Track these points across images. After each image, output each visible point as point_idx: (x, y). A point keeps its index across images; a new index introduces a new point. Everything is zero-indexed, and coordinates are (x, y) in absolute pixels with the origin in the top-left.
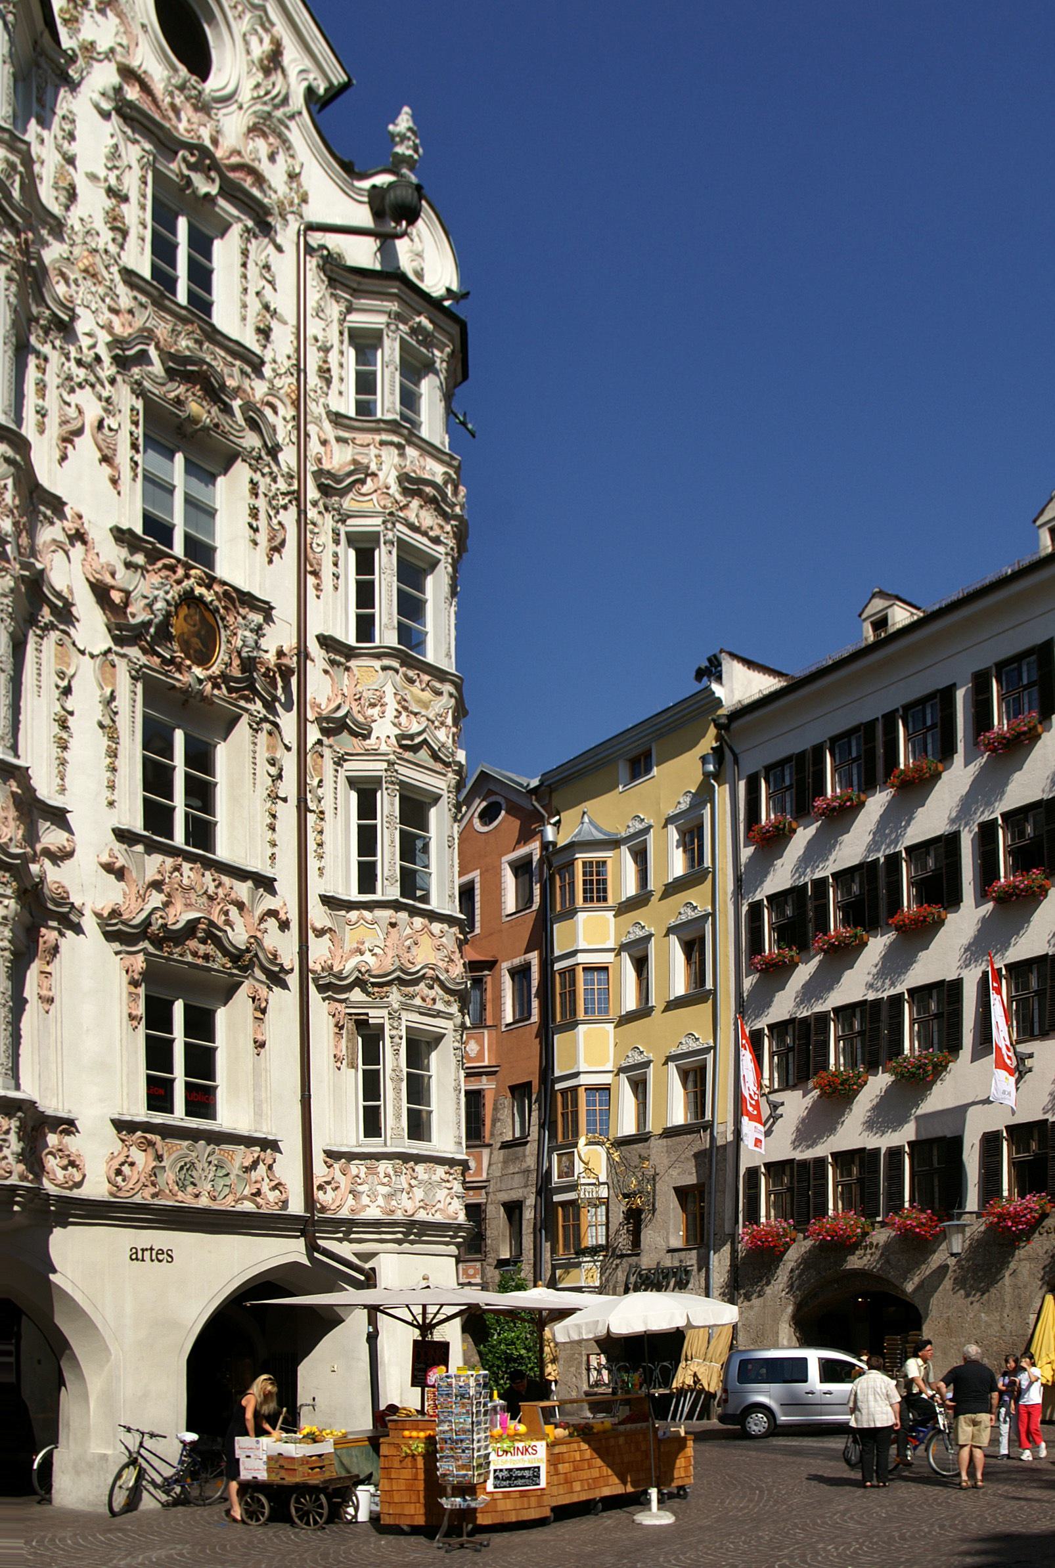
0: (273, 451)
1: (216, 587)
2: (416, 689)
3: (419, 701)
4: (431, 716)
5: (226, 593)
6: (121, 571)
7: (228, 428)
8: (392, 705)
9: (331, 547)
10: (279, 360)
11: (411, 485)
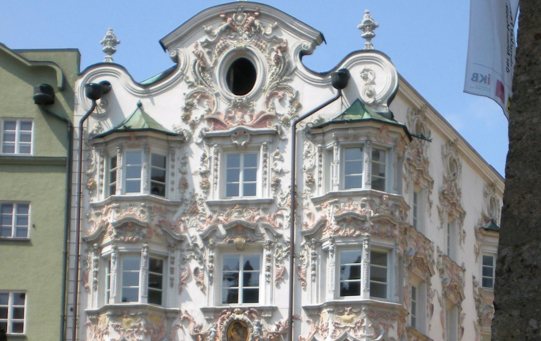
0: (280, 236)
1: (247, 312)
2: (346, 317)
3: (346, 321)
4: (353, 326)
5: (251, 312)
6: (205, 323)
7: (255, 238)
8: (331, 328)
9: (311, 263)
10: (284, 191)
11: (342, 220)
